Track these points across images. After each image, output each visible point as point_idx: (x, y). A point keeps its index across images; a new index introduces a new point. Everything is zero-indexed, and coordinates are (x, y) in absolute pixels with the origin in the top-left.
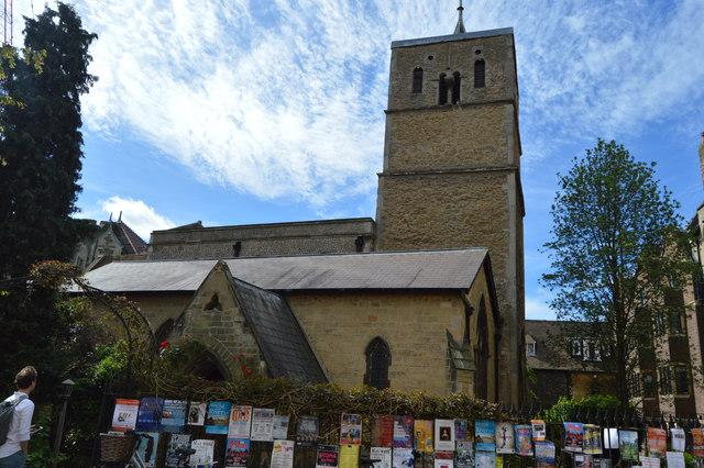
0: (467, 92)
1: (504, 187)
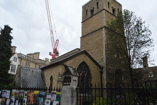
0: (95, 12)
1: (103, 32)
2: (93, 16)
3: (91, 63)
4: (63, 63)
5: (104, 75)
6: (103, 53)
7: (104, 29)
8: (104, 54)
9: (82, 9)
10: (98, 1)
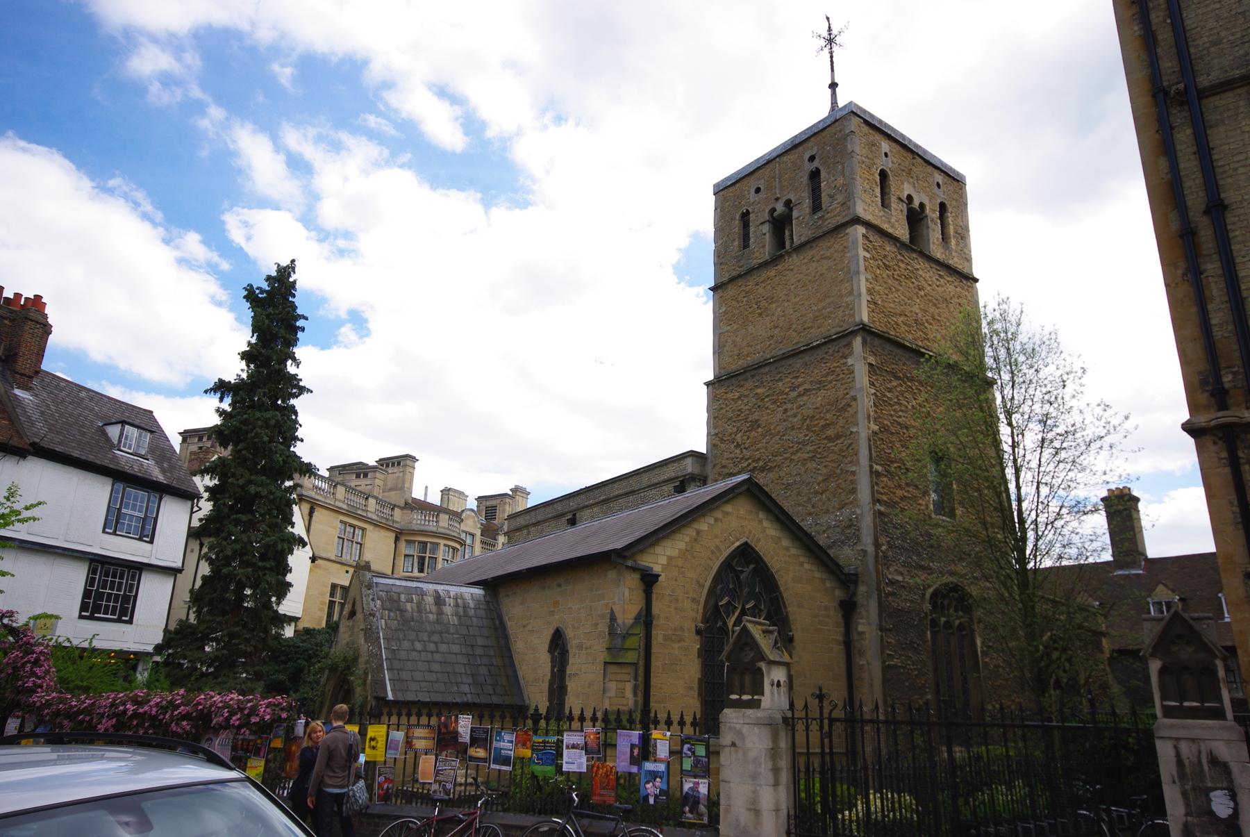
0: (799, 232)
1: (850, 361)
2: (789, 254)
3: (787, 549)
4: (630, 557)
5: (868, 625)
6: (853, 491)
7: (858, 342)
8: (864, 493)
9: (711, 199)
10: (816, 163)
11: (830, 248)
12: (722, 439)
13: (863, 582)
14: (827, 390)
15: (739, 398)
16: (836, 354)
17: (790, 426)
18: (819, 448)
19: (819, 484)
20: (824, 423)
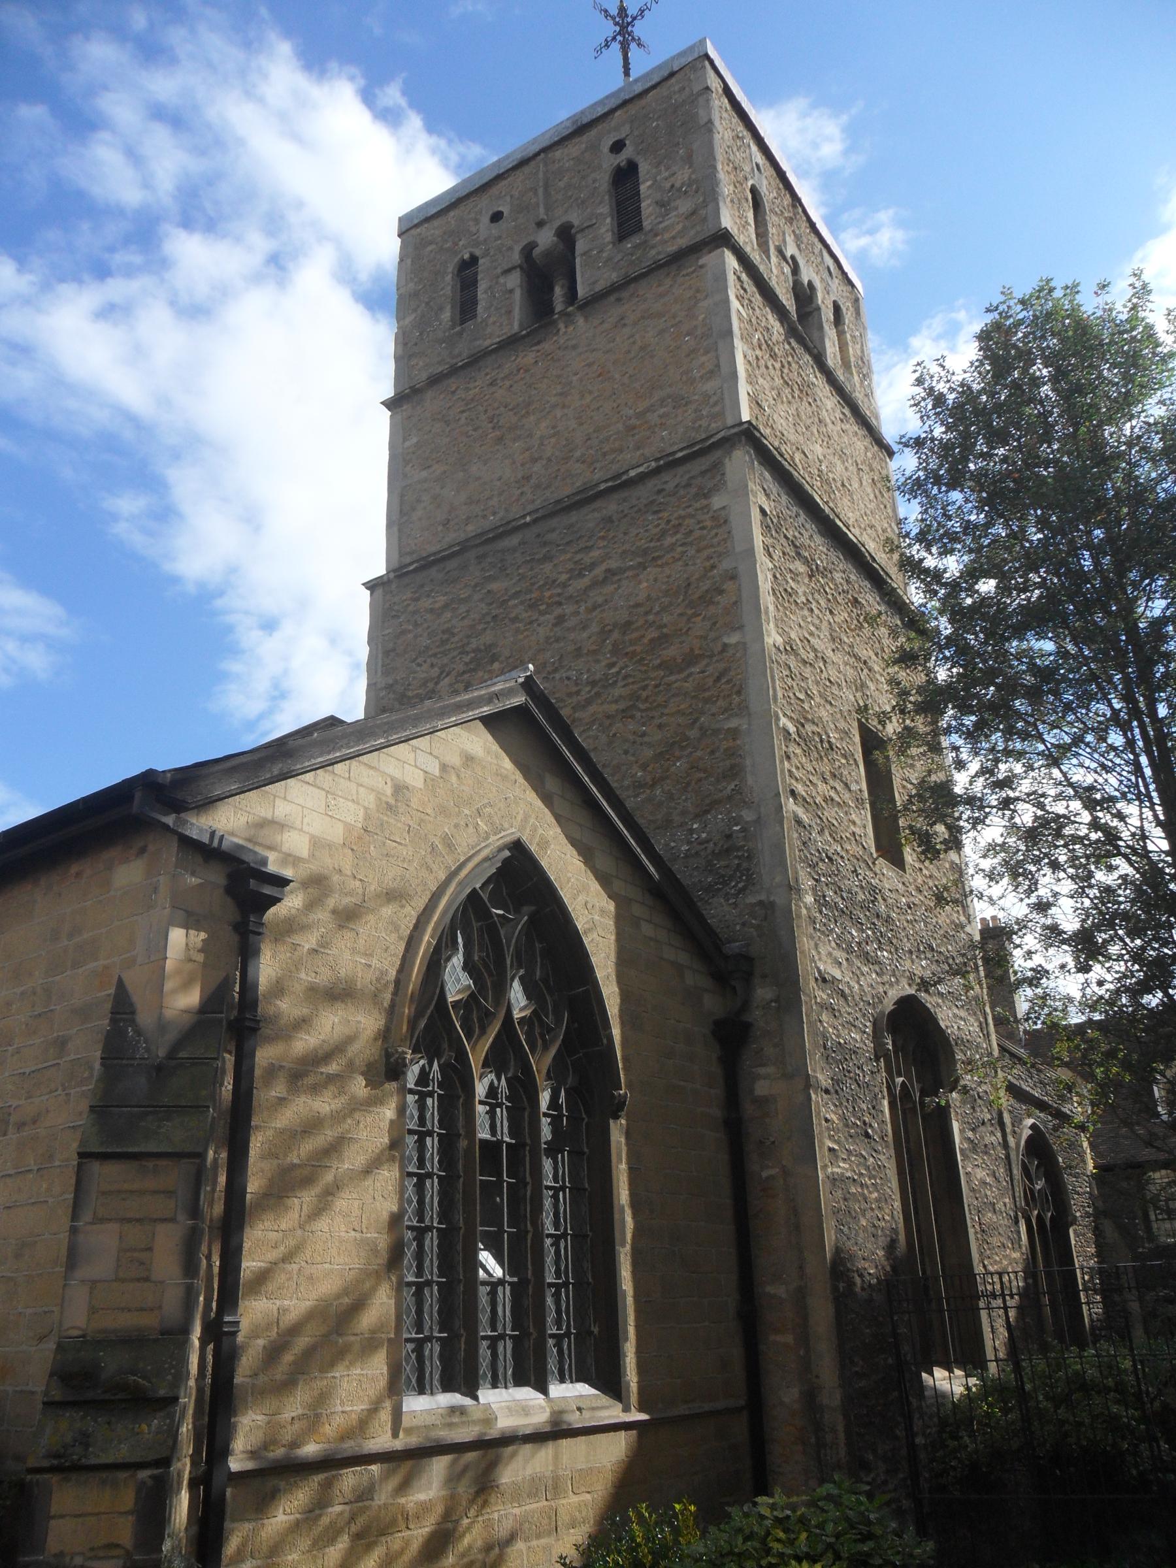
10: (628, 153)
11: (662, 295)
12: (403, 695)
13: (764, 976)
14: (661, 566)
15: (446, 606)
16: (682, 492)
17: (571, 648)
18: (644, 688)
19: (644, 767)
20: (655, 634)
